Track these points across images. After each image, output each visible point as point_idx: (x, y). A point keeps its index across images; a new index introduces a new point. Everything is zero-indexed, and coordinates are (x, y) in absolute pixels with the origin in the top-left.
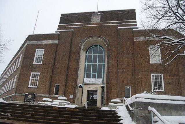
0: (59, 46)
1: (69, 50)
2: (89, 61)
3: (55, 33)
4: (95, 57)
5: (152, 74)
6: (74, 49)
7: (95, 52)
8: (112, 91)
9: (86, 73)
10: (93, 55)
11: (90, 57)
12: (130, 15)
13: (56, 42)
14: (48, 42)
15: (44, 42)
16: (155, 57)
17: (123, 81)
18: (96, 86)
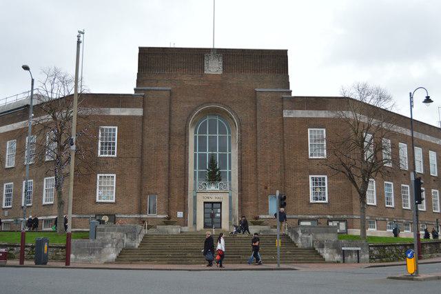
0: (146, 121)
1: (167, 130)
2: (202, 148)
3: (133, 92)
4: (212, 139)
5: (310, 176)
6: (178, 128)
7: (213, 131)
8: (249, 203)
9: (197, 170)
10: (208, 135)
11: (202, 139)
12: (276, 62)
13: (139, 112)
14: (125, 111)
15: (114, 112)
16: (317, 145)
17: (266, 188)
18: (219, 195)
